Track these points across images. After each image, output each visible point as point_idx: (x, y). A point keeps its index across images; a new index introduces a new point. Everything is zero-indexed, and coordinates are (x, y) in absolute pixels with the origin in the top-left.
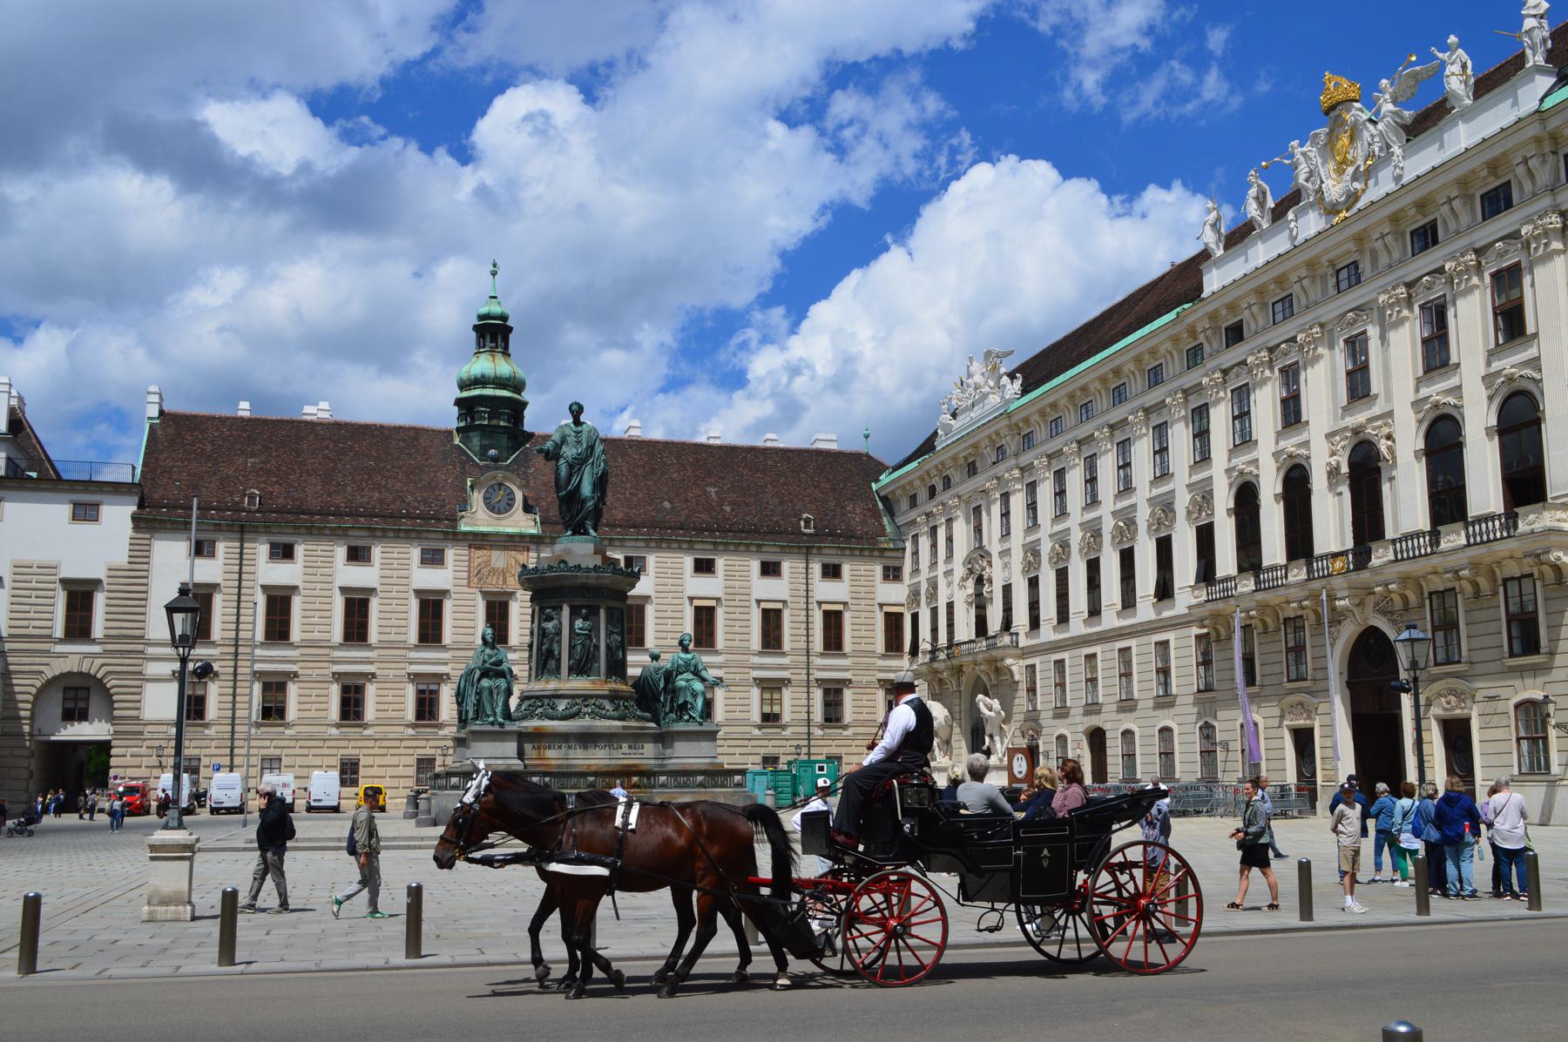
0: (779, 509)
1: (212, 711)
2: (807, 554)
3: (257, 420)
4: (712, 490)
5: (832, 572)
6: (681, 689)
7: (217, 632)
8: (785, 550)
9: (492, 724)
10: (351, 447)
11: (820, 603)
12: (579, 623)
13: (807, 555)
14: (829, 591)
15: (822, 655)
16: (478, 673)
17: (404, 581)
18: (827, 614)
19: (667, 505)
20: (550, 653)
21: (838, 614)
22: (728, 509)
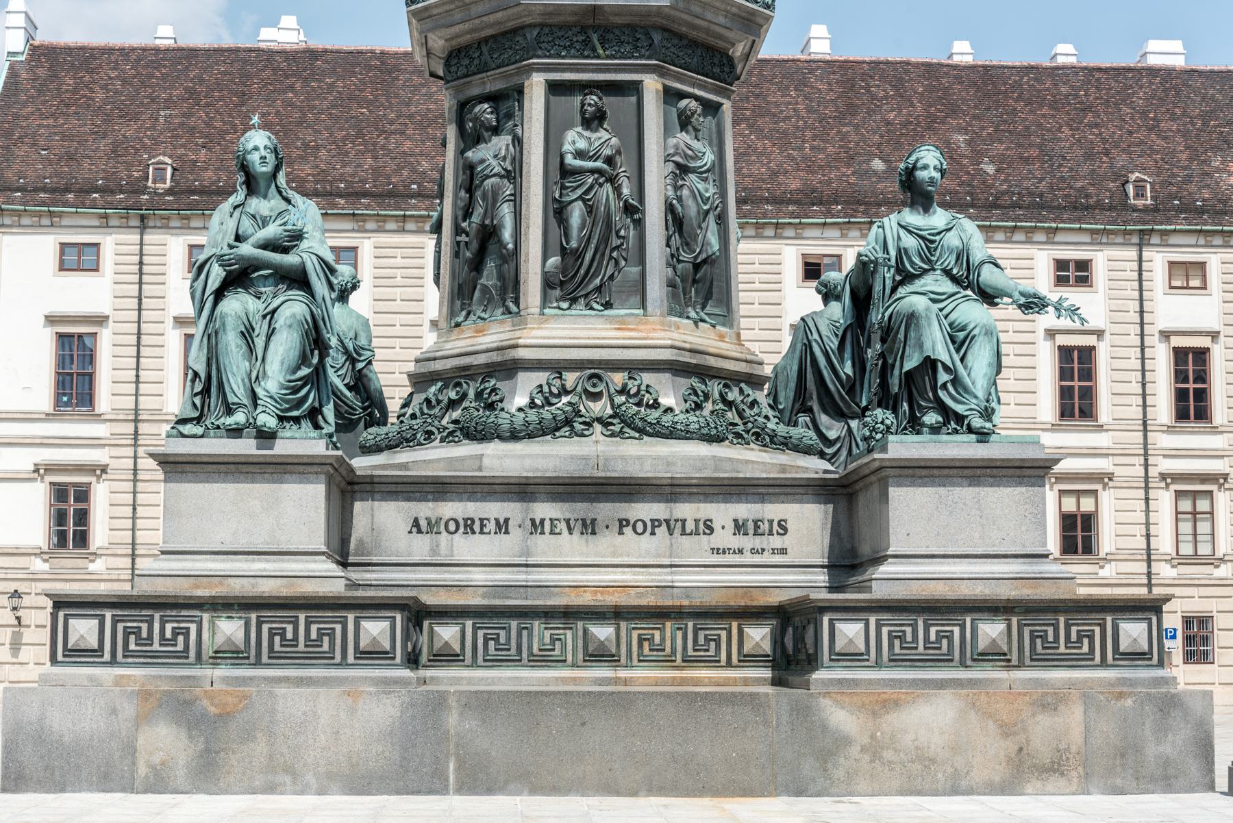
0: (1085, 169)
1: (99, 533)
2: (1143, 239)
3: (181, 49)
4: (961, 138)
5: (1188, 275)
6: (912, 318)
7: (104, 400)
8: (1099, 238)
9: (235, 432)
10: (332, 85)
11: (1166, 335)
12: (575, 139)
13: (1140, 246)
14: (1180, 312)
15: (1170, 430)
16: (217, 274)
17: (412, 307)
18: (1180, 355)
19: (878, 165)
20: (489, 234)
21: (1202, 355)
22: (990, 169)
